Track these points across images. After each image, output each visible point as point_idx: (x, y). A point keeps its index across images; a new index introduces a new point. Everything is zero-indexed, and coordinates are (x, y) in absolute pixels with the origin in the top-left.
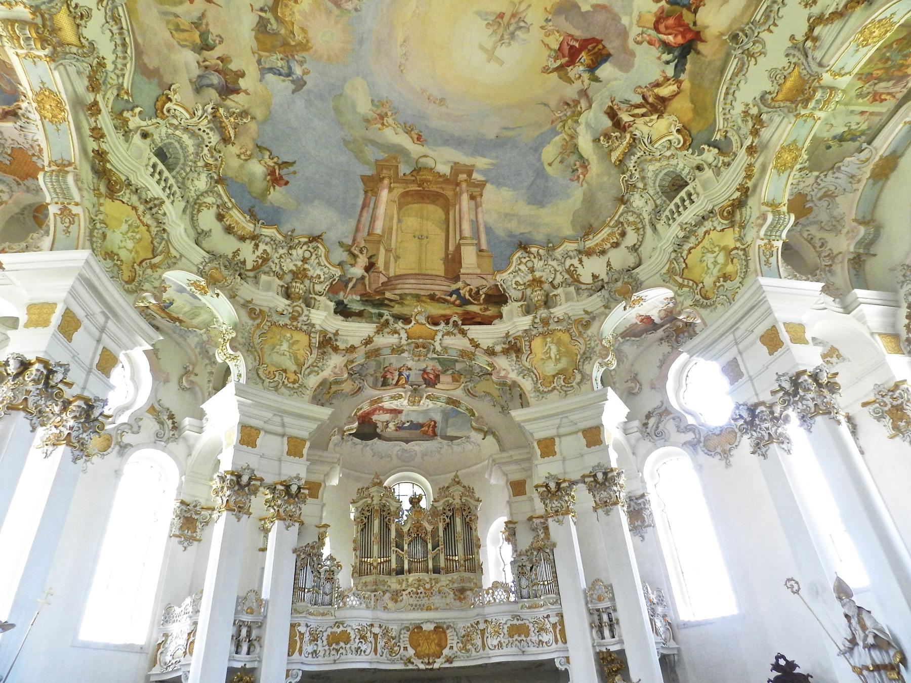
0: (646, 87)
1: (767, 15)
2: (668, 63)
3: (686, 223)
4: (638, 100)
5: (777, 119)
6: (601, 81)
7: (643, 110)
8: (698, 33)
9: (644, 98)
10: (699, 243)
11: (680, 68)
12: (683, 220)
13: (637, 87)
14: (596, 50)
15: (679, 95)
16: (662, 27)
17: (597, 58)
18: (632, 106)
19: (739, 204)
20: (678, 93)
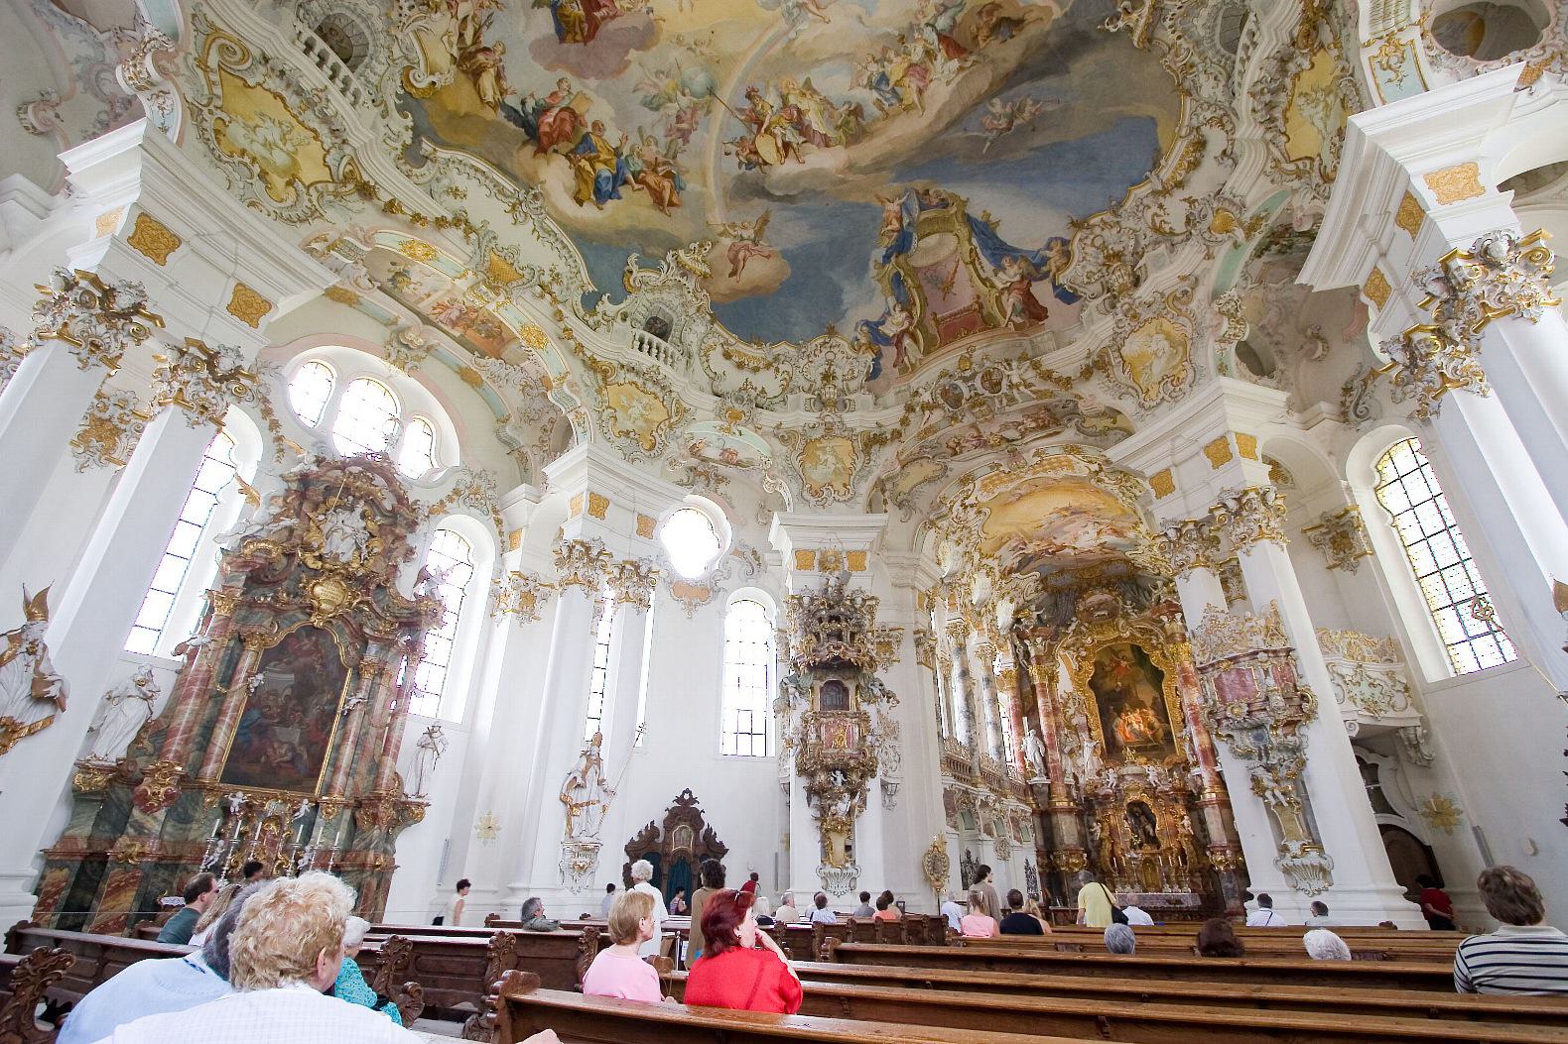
0: (501, 60)
1: (550, 233)
2: (523, 103)
3: (328, 100)
4: (487, 39)
5: (469, 249)
6: (533, 7)
7: (469, 40)
8: (545, 151)
9: (486, 49)
10: (294, 116)
11: (512, 114)
12: (333, 95)
13: (504, 49)
14: (578, 30)
15: (479, 102)
16: (566, 115)
17: (567, 23)
18: (480, 27)
19: (366, 191)
20: (482, 100)
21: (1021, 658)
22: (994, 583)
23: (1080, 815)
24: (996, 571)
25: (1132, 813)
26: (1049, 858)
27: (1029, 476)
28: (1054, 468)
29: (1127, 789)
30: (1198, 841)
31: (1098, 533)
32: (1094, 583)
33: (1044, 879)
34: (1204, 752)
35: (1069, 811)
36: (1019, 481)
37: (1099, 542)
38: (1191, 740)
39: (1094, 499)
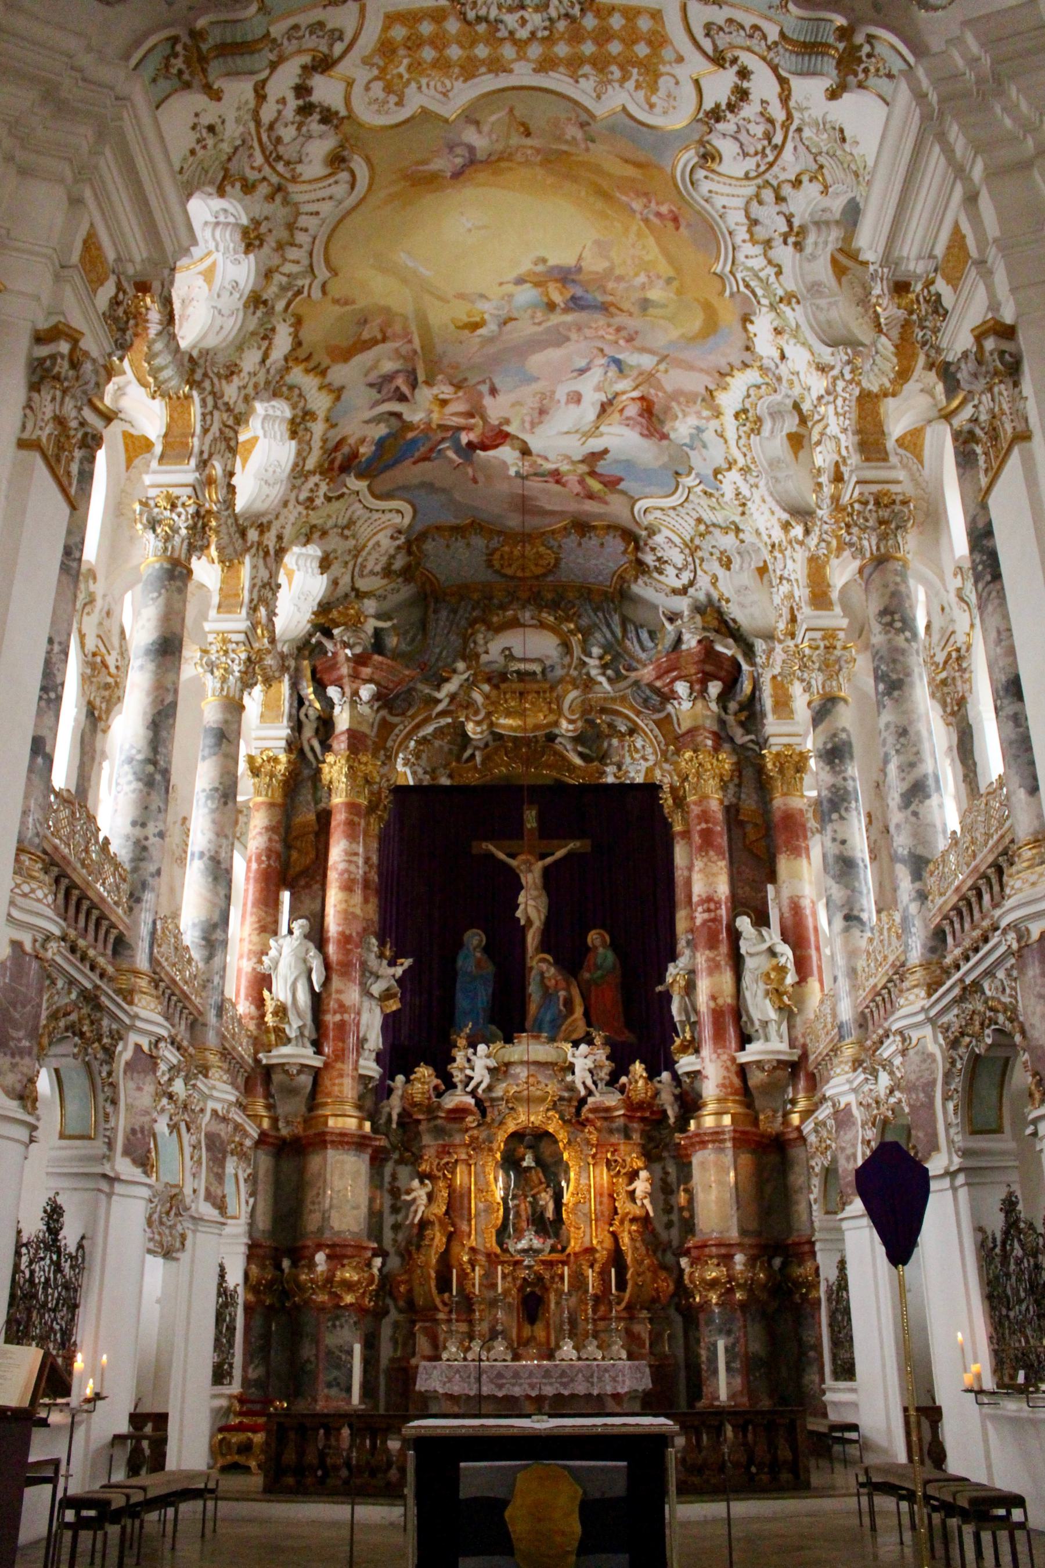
21: (308, 732)
22: (299, 473)
23: (378, 1160)
24: (318, 428)
25: (510, 1163)
26: (278, 1267)
27: (523, 74)
28: (601, 64)
29: (517, 1098)
30: (653, 1232)
31: (604, 408)
32: (524, 595)
33: (258, 1321)
34: (717, 1015)
35: (360, 1143)
36: (487, 83)
37: (595, 444)
38: (690, 988)
39: (652, 251)
